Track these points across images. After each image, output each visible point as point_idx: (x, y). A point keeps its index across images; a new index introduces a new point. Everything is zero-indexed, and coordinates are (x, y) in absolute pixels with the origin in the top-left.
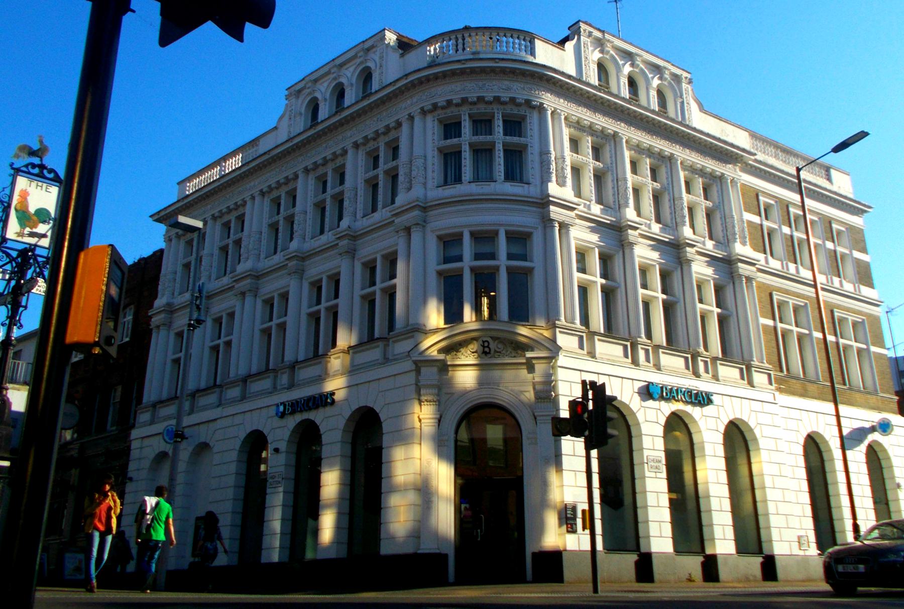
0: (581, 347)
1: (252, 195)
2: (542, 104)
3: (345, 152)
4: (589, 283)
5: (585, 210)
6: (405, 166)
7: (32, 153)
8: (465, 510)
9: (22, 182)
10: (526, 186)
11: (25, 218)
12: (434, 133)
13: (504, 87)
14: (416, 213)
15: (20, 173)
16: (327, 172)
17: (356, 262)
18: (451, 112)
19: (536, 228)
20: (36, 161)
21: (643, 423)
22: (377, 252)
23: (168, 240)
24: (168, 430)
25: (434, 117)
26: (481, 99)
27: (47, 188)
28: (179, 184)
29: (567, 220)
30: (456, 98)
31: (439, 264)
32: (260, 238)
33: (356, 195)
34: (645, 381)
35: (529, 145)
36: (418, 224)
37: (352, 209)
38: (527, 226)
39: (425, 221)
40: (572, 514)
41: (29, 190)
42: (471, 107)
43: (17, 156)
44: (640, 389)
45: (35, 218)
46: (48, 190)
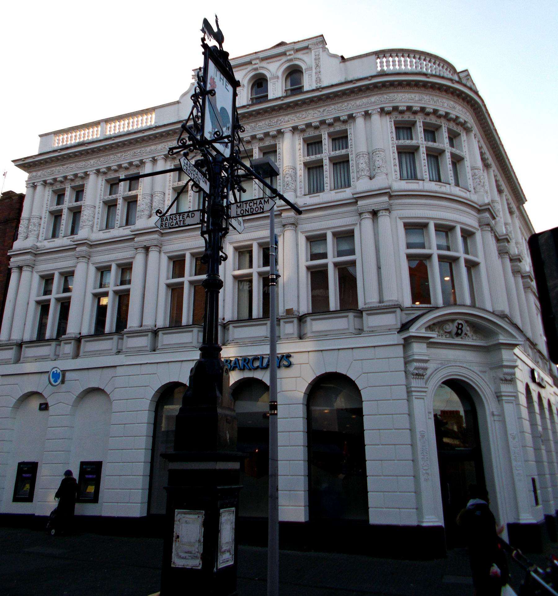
1: (153, 158)
3: (280, 133)
6: (364, 155)
10: (468, 193)
12: (392, 132)
13: (450, 106)
14: (386, 199)
16: (252, 149)
18: (408, 117)
22: (328, 229)
23: (33, 186)
24: (53, 372)
25: (390, 118)
26: (435, 112)
28: (41, 136)
30: (416, 107)
32: (164, 198)
33: (296, 173)
35: (465, 159)
37: (293, 185)
42: (426, 117)
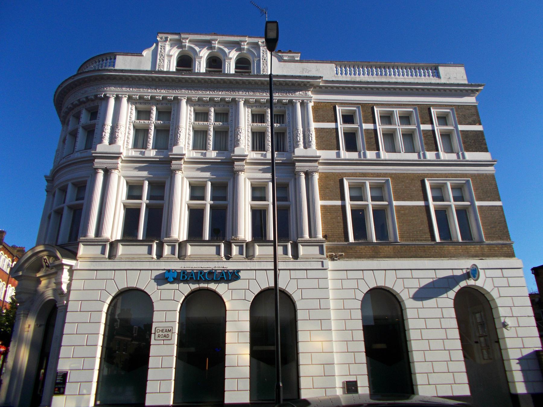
2: (105, 95)
5: (141, 156)
19: (88, 177)
29: (108, 166)
34: (164, 270)
40: (61, 380)
44: (156, 276)
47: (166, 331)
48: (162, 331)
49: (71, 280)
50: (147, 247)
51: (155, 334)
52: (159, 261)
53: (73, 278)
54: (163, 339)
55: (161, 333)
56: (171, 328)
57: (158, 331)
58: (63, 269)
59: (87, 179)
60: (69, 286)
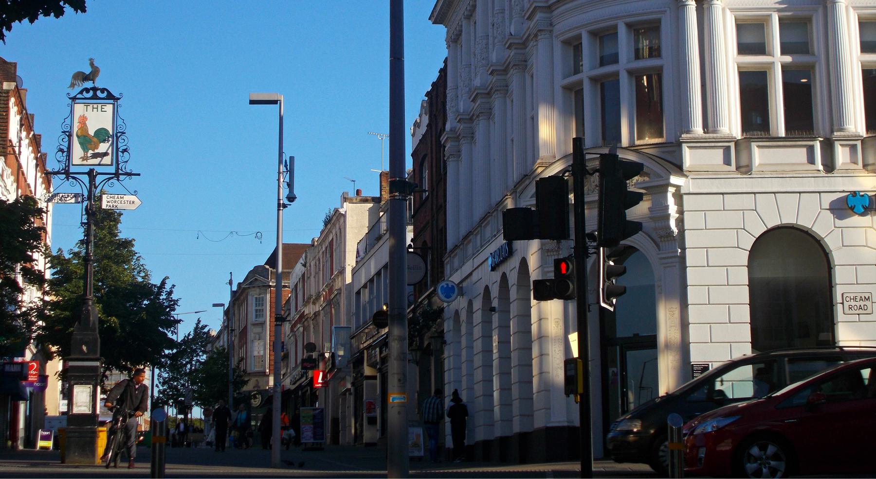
0: (727, 162)
4: (769, 65)
7: (85, 78)
8: (612, 376)
9: (79, 109)
11: (87, 142)
14: (538, 16)
15: (77, 101)
17: (527, 75)
19: (664, 12)
20: (89, 84)
21: (839, 248)
27: (102, 108)
31: (564, 78)
32: (487, 44)
34: (844, 191)
36: (540, 31)
38: (639, 14)
39: (551, 25)
41: (87, 114)
43: (72, 85)
45: (95, 140)
46: (103, 110)
47: (861, 299)
48: (855, 299)
49: (681, 212)
50: (804, 150)
51: (843, 303)
52: (833, 175)
53: (685, 208)
54: (857, 312)
55: (853, 303)
56: (869, 295)
57: (848, 299)
58: (666, 191)
59: (658, 16)
60: (680, 222)
